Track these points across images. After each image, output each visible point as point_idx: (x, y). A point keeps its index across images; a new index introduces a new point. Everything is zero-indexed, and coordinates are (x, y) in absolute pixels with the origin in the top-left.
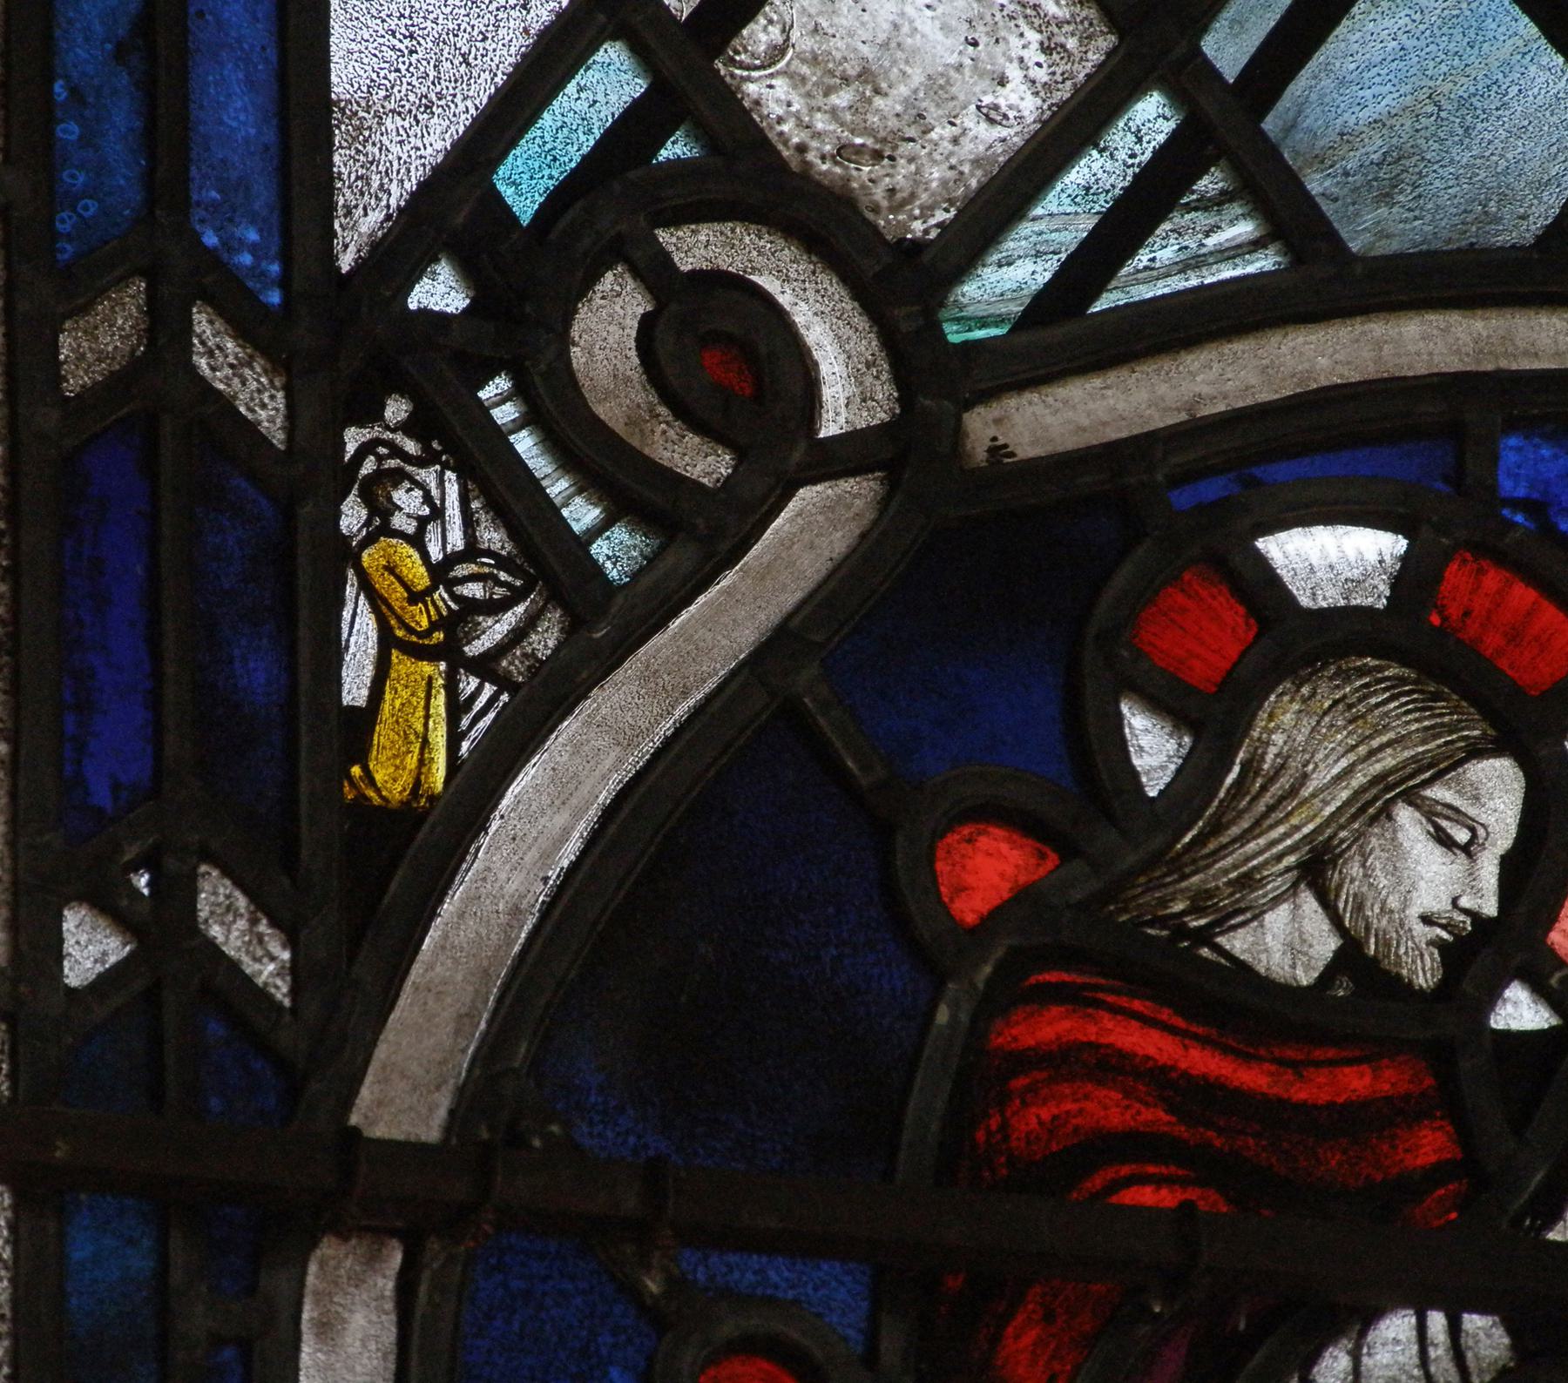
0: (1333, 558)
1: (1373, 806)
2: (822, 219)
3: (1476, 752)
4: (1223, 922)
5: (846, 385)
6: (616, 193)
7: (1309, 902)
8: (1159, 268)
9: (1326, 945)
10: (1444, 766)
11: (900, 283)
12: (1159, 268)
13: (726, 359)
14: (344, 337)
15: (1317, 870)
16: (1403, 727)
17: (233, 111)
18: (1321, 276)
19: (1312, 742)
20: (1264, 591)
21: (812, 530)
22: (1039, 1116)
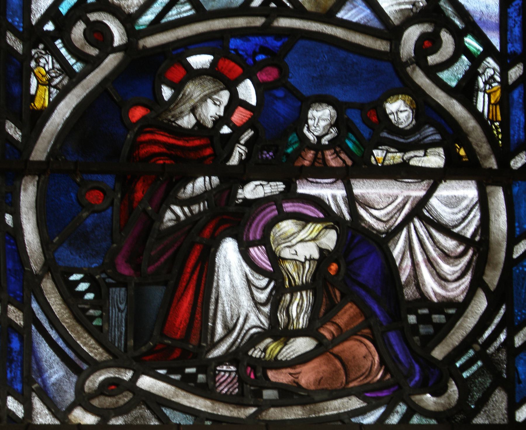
0: (200, 61)
1: (203, 100)
2: (117, 12)
3: (222, 90)
4: (177, 119)
7: (192, 115)
8: (173, 15)
9: (193, 121)
10: (216, 92)
11: (129, 20)
12: (173, 15)
13: (99, 35)
15: (193, 110)
16: (209, 86)
19: (194, 90)
20: (188, 66)
22: (144, 151)
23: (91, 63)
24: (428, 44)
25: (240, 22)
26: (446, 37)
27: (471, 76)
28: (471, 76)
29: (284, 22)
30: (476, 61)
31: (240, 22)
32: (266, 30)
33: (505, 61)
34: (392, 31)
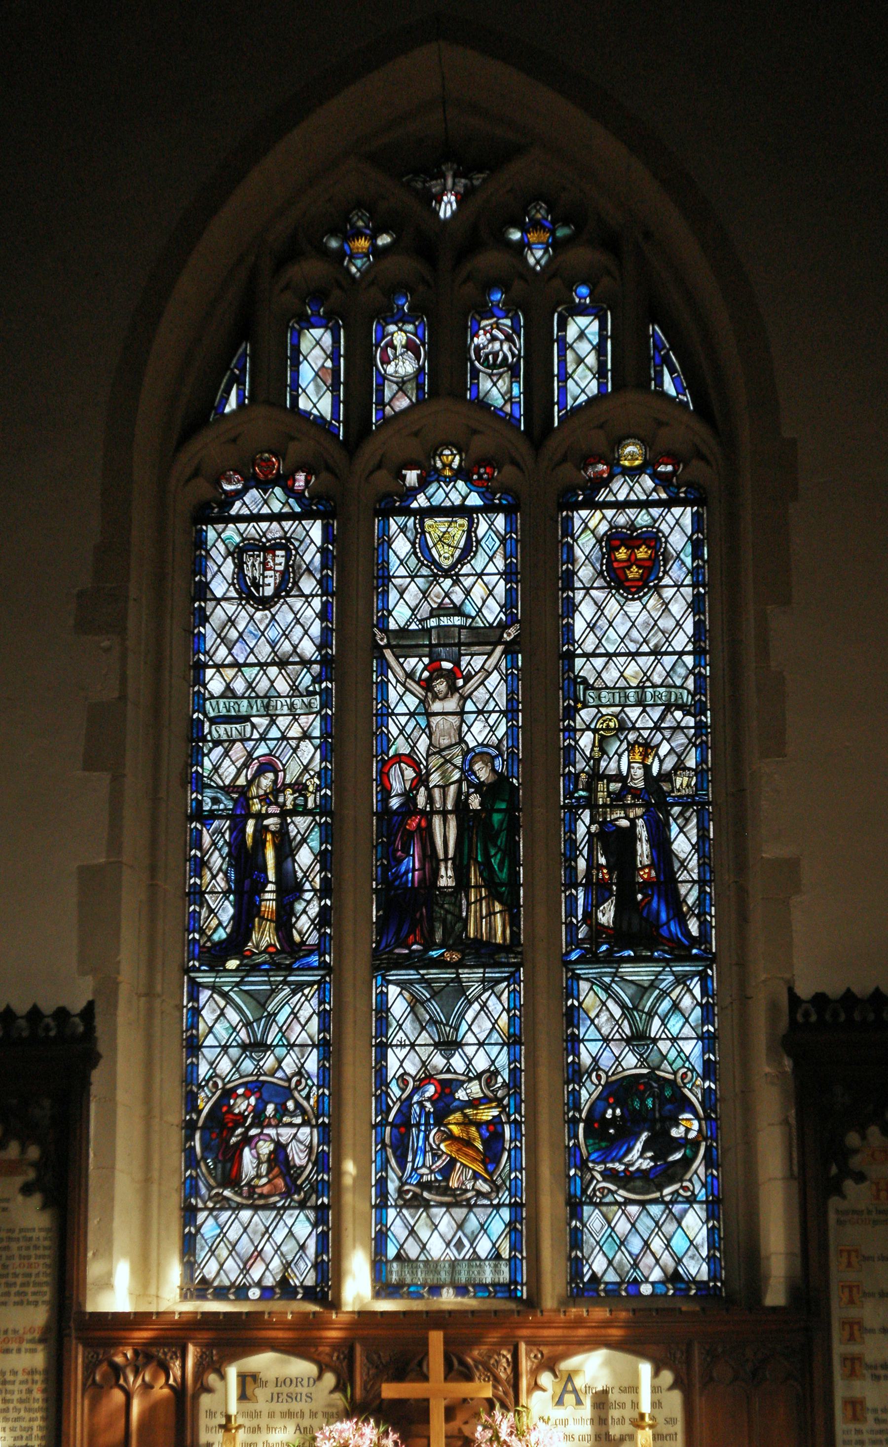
5: (220, 1085)
6: (211, 1077)
11: (223, 1080)
13: (215, 1084)
14: (200, 1087)
17: (195, 1075)
18: (241, 1077)
21: (219, 1093)
23: (214, 1094)
24: (299, 1083)
25: (250, 1079)
26: (303, 1080)
27: (309, 1093)
28: (309, 1093)
29: (262, 1078)
30: (311, 1088)
31: (250, 1079)
32: (257, 1081)
33: (319, 1087)
34: (289, 1080)
